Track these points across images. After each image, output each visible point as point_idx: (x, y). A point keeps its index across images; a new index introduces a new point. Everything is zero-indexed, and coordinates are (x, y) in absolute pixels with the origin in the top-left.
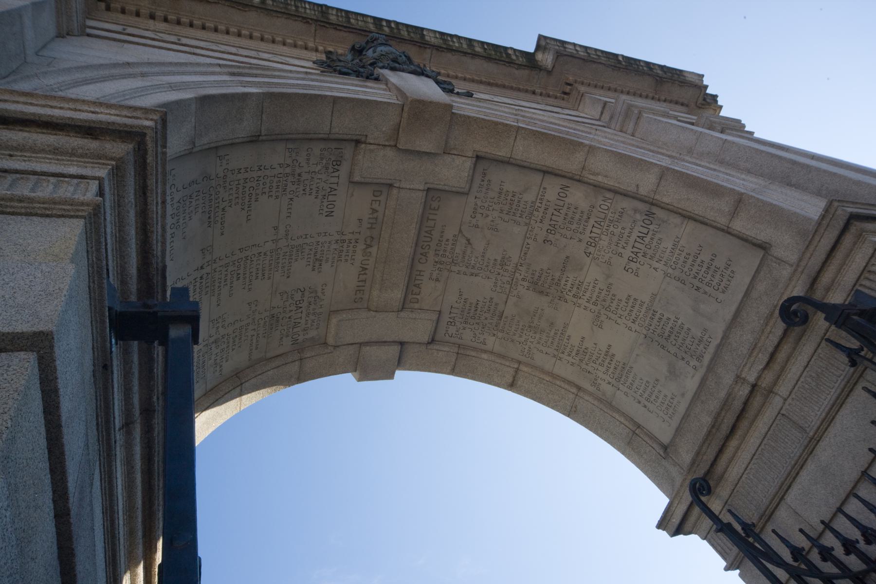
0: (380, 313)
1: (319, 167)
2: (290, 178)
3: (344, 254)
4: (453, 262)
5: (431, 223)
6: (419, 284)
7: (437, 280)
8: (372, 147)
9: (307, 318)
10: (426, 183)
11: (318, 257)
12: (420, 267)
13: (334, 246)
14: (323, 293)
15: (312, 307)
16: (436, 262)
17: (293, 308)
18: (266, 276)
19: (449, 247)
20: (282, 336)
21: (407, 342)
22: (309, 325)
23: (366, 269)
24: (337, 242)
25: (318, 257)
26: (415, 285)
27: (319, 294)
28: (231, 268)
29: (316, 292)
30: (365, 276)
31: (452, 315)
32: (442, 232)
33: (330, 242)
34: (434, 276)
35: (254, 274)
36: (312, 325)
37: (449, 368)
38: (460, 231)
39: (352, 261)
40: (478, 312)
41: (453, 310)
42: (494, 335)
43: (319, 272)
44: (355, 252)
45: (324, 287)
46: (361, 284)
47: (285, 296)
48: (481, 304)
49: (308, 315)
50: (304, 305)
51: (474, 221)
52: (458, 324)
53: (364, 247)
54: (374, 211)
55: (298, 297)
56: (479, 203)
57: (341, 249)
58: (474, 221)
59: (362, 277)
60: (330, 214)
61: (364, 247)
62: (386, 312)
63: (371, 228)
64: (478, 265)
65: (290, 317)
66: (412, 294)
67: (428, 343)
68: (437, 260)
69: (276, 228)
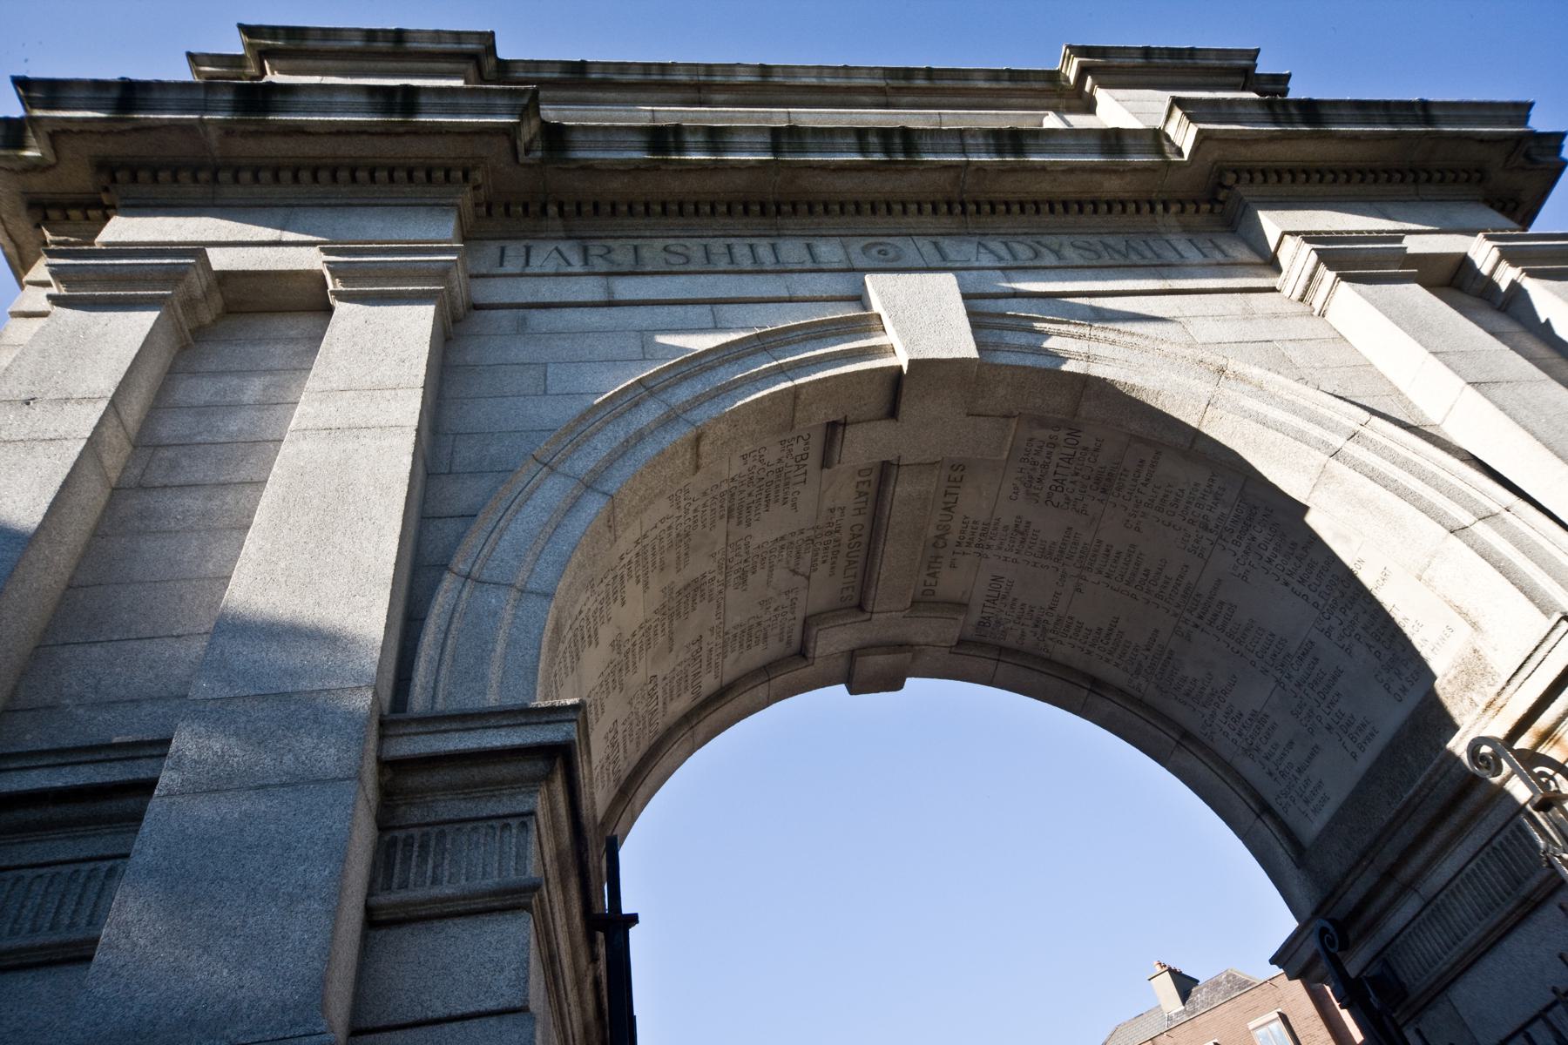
0: (928, 461)
1: (1009, 625)
2: (1051, 627)
3: (979, 531)
4: (813, 540)
5: (850, 572)
6: (860, 496)
7: (832, 510)
8: (943, 644)
9: (1047, 460)
10: (870, 619)
11: (1019, 537)
12: (860, 519)
13: (995, 543)
14: (1016, 488)
15: (1037, 475)
16: (837, 532)
17: (1067, 485)
18: (1103, 547)
19: (821, 554)
20: (1096, 454)
21: (879, 420)
22: (1046, 450)
23: (944, 509)
24: (989, 547)
25: (1019, 537)
26: (866, 494)
27: (1022, 489)
28: (1157, 589)
29: (1028, 493)
30: (947, 500)
31: (803, 471)
32: (833, 568)
33: (1000, 548)
34: (837, 513)
35: (1122, 561)
36: (1041, 447)
37: (802, 397)
38: (808, 578)
39: (966, 520)
40: (763, 496)
41: (802, 478)
42: (733, 479)
43: (1019, 517)
44: (963, 532)
45: (1014, 495)
46: (954, 490)
47: (1080, 506)
48: (763, 508)
49: (1045, 466)
50: (1048, 482)
51: (792, 595)
52: (792, 462)
53: (947, 537)
54: (933, 575)
55: (1058, 497)
56: (790, 616)
57: (983, 538)
58: (792, 595)
59: (951, 499)
60: (996, 579)
61: (947, 537)
62: (919, 464)
63: (938, 557)
64: (777, 554)
65: (1077, 474)
66: (870, 481)
67: (845, 424)
68: (837, 535)
69: (1079, 590)
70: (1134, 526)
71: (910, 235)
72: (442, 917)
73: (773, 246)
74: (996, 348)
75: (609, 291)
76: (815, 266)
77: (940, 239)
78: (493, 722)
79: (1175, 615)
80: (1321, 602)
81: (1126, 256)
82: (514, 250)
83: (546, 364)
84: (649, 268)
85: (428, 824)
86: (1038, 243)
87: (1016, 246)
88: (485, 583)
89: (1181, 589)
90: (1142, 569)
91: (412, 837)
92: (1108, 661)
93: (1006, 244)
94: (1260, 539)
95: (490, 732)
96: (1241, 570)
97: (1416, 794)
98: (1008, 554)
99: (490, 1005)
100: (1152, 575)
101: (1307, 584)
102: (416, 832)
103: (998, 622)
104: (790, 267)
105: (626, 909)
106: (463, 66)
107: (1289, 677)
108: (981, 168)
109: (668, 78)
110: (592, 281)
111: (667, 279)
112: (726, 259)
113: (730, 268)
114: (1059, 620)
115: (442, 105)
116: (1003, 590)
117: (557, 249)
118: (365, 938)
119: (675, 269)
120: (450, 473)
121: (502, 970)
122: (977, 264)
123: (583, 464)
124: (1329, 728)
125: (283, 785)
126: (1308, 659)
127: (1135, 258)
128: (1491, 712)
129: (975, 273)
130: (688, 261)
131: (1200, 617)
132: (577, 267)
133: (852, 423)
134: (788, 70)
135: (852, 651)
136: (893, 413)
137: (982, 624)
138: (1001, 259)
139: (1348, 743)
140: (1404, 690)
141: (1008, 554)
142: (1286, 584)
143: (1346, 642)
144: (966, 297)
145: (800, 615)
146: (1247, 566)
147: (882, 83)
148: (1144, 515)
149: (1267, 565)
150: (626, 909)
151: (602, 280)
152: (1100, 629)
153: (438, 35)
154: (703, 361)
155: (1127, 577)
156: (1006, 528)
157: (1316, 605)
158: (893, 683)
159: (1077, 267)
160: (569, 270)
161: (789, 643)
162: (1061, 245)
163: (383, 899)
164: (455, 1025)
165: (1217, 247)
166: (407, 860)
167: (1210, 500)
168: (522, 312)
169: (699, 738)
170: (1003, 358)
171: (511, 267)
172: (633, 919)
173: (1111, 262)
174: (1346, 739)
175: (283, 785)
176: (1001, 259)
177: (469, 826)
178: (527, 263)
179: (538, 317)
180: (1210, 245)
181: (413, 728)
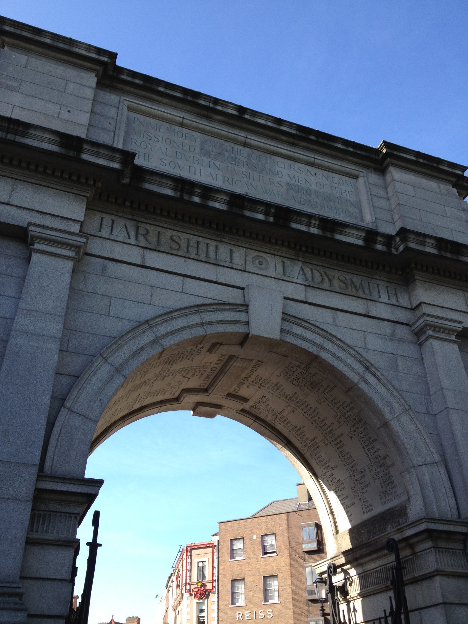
14: (281, 374)
17: (300, 380)
18: (306, 404)
22: (296, 368)
28: (321, 425)
33: (268, 388)
34: (208, 364)
49: (294, 372)
51: (180, 383)
65: (304, 379)
70: (320, 403)
71: (274, 255)
72: (47, 544)
73: (217, 247)
74: (288, 332)
75: (143, 260)
76: (230, 265)
77: (286, 260)
78: (73, 482)
79: (324, 436)
80: (372, 460)
81: (357, 291)
82: (107, 219)
83: (111, 297)
84: (162, 249)
85: (46, 511)
86: (325, 273)
87: (315, 272)
88: (74, 412)
89: (329, 429)
90: (318, 416)
91: (40, 514)
92: (296, 437)
93: (312, 270)
94: (361, 429)
95: (72, 486)
96: (351, 435)
97: (371, 541)
98: (270, 391)
99: (59, 577)
100: (321, 420)
101: (370, 452)
102: (42, 512)
103: (259, 409)
104: (220, 263)
105: (98, 542)
106: (98, 68)
107: (354, 476)
108: (313, 235)
109: (196, 100)
110: (137, 250)
111: (169, 256)
112: (195, 251)
113: (196, 257)
114: (282, 417)
115: (92, 151)
116: (264, 400)
117: (125, 225)
118: (25, 550)
119: (173, 252)
120: (67, 351)
121: (64, 567)
122: (296, 281)
123: (117, 360)
124: (360, 499)
125: (9, 499)
126: (362, 475)
127: (360, 293)
128: (399, 531)
129: (294, 284)
130: (179, 249)
131: (333, 441)
132: (132, 241)
133: (223, 345)
134: (254, 113)
135: (198, 403)
136: (242, 344)
137: (253, 407)
138: (307, 280)
139: (364, 508)
140: (385, 502)
141: (270, 391)
142: (364, 448)
143: (375, 477)
144: (283, 313)
145: (181, 388)
146: (353, 435)
147: (293, 132)
148: (324, 401)
149: (360, 439)
150: (98, 542)
151: (141, 250)
152: (296, 427)
153: (89, 47)
154: (173, 315)
155: (312, 416)
156: (273, 383)
157: (370, 460)
158: (211, 416)
159: (336, 292)
160: (129, 241)
161: (173, 395)
162: (334, 277)
163: (31, 536)
164: (49, 582)
165: (396, 295)
166: (38, 522)
167: (348, 409)
168: (106, 261)
169: (125, 424)
170: (290, 339)
171: (105, 233)
172: (100, 545)
173: (350, 293)
174: (364, 506)
175: (9, 499)
176: (307, 280)
177: (58, 514)
178: (111, 233)
179: (112, 266)
180: (394, 292)
181: (47, 479)
